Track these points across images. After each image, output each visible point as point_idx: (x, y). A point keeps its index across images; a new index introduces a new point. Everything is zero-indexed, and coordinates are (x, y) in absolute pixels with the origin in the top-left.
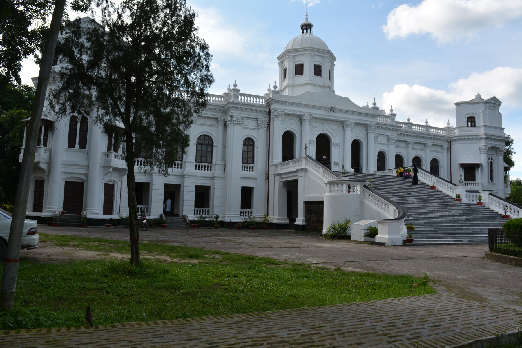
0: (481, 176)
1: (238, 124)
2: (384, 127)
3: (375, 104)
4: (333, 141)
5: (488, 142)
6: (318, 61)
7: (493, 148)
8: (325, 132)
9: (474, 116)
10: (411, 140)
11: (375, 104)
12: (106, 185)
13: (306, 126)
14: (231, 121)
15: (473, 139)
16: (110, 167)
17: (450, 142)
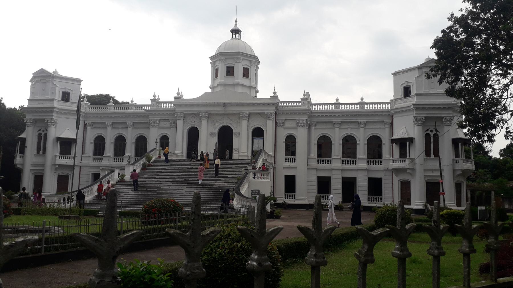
0: (417, 151)
1: (154, 126)
2: (290, 112)
3: (275, 93)
4: (234, 131)
5: (419, 112)
6: (230, 63)
7: (427, 118)
8: (225, 124)
9: (409, 84)
10: (338, 120)
11: (275, 93)
12: (59, 177)
13: (204, 123)
14: (150, 124)
15: (406, 111)
16: (55, 165)
17: (392, 117)
